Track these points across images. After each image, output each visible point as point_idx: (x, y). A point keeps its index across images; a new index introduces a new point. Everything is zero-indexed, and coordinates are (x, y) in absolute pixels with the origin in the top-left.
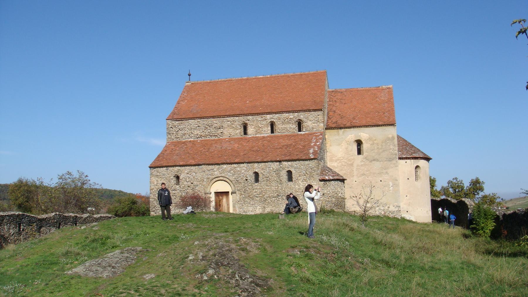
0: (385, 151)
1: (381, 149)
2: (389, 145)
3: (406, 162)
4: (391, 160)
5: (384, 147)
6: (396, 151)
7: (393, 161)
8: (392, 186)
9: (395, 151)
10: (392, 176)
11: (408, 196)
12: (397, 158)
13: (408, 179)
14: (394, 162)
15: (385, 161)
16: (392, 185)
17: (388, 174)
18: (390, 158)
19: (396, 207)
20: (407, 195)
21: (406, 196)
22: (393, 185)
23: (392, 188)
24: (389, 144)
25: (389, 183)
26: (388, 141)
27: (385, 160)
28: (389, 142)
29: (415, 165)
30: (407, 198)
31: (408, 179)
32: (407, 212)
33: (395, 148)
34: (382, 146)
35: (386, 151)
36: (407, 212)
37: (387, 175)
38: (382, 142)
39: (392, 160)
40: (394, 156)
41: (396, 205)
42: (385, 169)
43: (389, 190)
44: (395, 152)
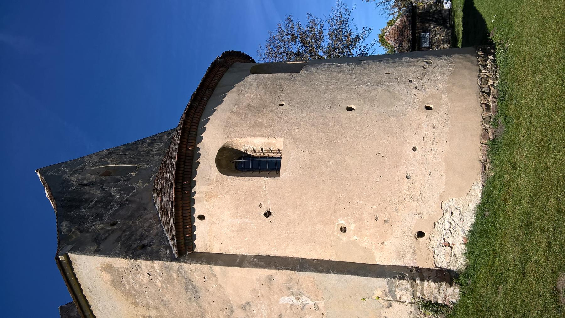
0: (163, 301)
1: (157, 309)
2: (140, 285)
3: (202, 218)
4: (190, 287)
5: (151, 302)
6: (154, 267)
7: (195, 283)
8: (298, 299)
9: (155, 271)
10: (254, 290)
11: (342, 222)
12: (181, 267)
13: (268, 214)
14: (197, 279)
15: (199, 306)
16: (293, 299)
17: (248, 303)
18: (187, 289)
19: (394, 296)
20: (337, 228)
21: (345, 231)
22: (292, 294)
23: (303, 298)
24: (136, 286)
25: (285, 305)
26: (128, 287)
27: (194, 304)
28: (129, 284)
29: (215, 172)
30: (351, 228)
31: (268, 214)
32: (421, 234)
33: (144, 268)
34: (148, 307)
35: (165, 299)
36: (421, 234)
37: (253, 308)
38: (136, 304)
39: (191, 285)
40: (175, 275)
41: (386, 295)
42: (232, 312)
43: (313, 308)
44: (157, 268)
